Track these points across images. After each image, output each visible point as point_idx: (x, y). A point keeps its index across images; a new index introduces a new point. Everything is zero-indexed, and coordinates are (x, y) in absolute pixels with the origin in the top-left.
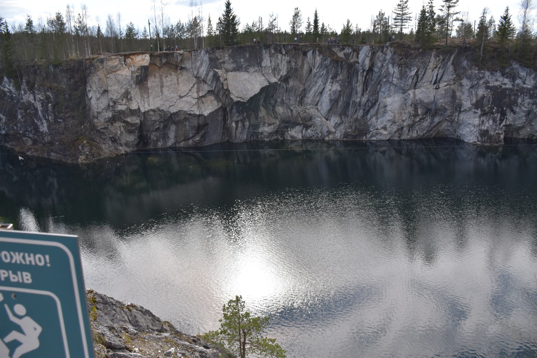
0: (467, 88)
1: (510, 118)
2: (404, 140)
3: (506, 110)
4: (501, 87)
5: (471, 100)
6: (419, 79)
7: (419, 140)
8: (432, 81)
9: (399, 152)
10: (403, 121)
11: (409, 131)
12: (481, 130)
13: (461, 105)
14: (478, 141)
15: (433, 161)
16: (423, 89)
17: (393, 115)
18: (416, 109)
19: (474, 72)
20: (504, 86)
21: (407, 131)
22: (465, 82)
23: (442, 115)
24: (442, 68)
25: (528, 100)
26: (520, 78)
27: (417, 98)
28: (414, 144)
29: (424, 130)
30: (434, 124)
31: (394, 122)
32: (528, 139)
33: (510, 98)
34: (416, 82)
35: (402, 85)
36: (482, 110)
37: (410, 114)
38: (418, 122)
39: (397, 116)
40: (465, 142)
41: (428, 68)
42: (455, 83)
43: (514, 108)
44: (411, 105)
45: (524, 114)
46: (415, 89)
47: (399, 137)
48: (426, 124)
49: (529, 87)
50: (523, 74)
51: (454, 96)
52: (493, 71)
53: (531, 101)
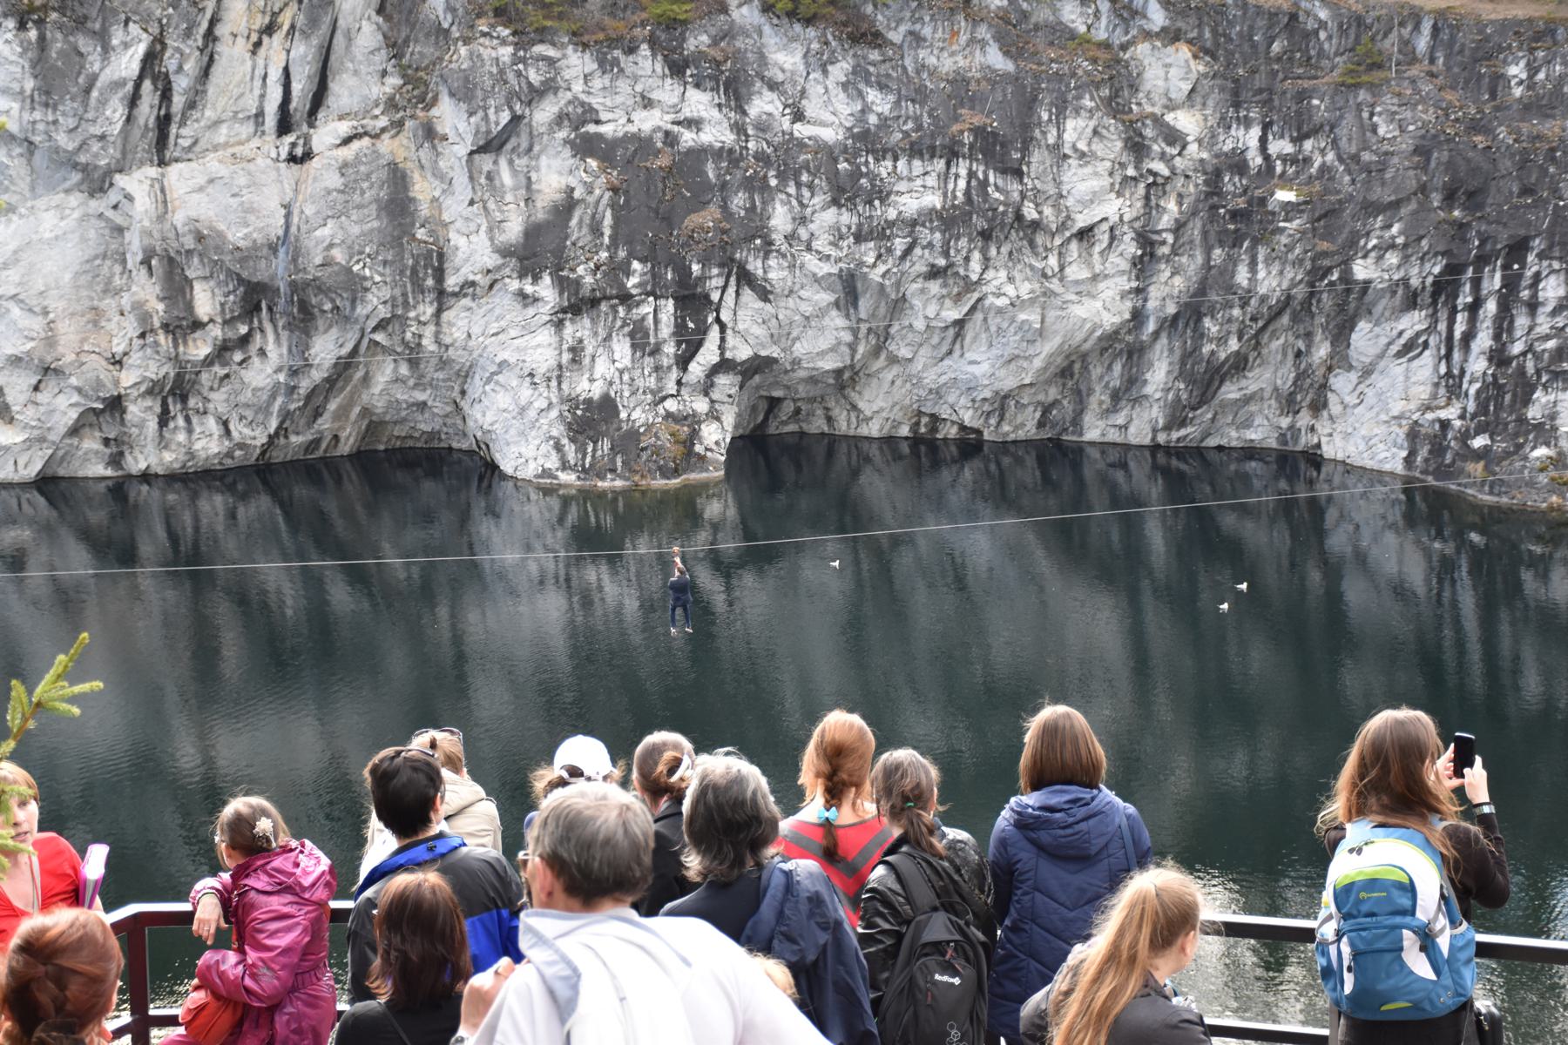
0: (462, 150)
1: (745, 327)
2: (146, 477)
3: (702, 279)
4: (670, 139)
5: (495, 227)
6: (178, 101)
7: (256, 475)
8: (259, 115)
9: (116, 550)
10: (117, 362)
11: (164, 419)
12: (572, 401)
13: (441, 256)
14: (565, 466)
15: (341, 596)
16: (213, 164)
17: (36, 324)
18: (177, 288)
19: (487, 53)
20: (688, 138)
21: (152, 424)
22: (449, 115)
23: (342, 317)
24: (306, 35)
25: (830, 216)
26: (773, 86)
27: (179, 218)
28: (214, 505)
29: (265, 410)
30: (317, 375)
31: (48, 371)
32: (916, 440)
33: (725, 207)
34: (164, 122)
35: (64, 141)
36: (562, 284)
37: (144, 318)
38: (208, 362)
39: (69, 334)
40: (504, 477)
41: (222, 30)
42: (399, 125)
43: (755, 266)
44: (146, 262)
45: (826, 298)
46: (162, 163)
47: (116, 460)
48: (263, 371)
49: (829, 135)
50: (785, 56)
51: (398, 205)
52: (608, 48)
53: (846, 218)
